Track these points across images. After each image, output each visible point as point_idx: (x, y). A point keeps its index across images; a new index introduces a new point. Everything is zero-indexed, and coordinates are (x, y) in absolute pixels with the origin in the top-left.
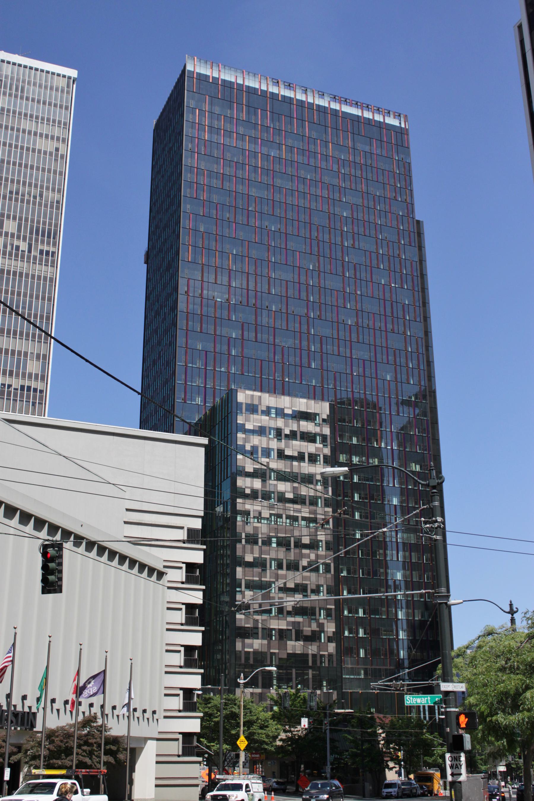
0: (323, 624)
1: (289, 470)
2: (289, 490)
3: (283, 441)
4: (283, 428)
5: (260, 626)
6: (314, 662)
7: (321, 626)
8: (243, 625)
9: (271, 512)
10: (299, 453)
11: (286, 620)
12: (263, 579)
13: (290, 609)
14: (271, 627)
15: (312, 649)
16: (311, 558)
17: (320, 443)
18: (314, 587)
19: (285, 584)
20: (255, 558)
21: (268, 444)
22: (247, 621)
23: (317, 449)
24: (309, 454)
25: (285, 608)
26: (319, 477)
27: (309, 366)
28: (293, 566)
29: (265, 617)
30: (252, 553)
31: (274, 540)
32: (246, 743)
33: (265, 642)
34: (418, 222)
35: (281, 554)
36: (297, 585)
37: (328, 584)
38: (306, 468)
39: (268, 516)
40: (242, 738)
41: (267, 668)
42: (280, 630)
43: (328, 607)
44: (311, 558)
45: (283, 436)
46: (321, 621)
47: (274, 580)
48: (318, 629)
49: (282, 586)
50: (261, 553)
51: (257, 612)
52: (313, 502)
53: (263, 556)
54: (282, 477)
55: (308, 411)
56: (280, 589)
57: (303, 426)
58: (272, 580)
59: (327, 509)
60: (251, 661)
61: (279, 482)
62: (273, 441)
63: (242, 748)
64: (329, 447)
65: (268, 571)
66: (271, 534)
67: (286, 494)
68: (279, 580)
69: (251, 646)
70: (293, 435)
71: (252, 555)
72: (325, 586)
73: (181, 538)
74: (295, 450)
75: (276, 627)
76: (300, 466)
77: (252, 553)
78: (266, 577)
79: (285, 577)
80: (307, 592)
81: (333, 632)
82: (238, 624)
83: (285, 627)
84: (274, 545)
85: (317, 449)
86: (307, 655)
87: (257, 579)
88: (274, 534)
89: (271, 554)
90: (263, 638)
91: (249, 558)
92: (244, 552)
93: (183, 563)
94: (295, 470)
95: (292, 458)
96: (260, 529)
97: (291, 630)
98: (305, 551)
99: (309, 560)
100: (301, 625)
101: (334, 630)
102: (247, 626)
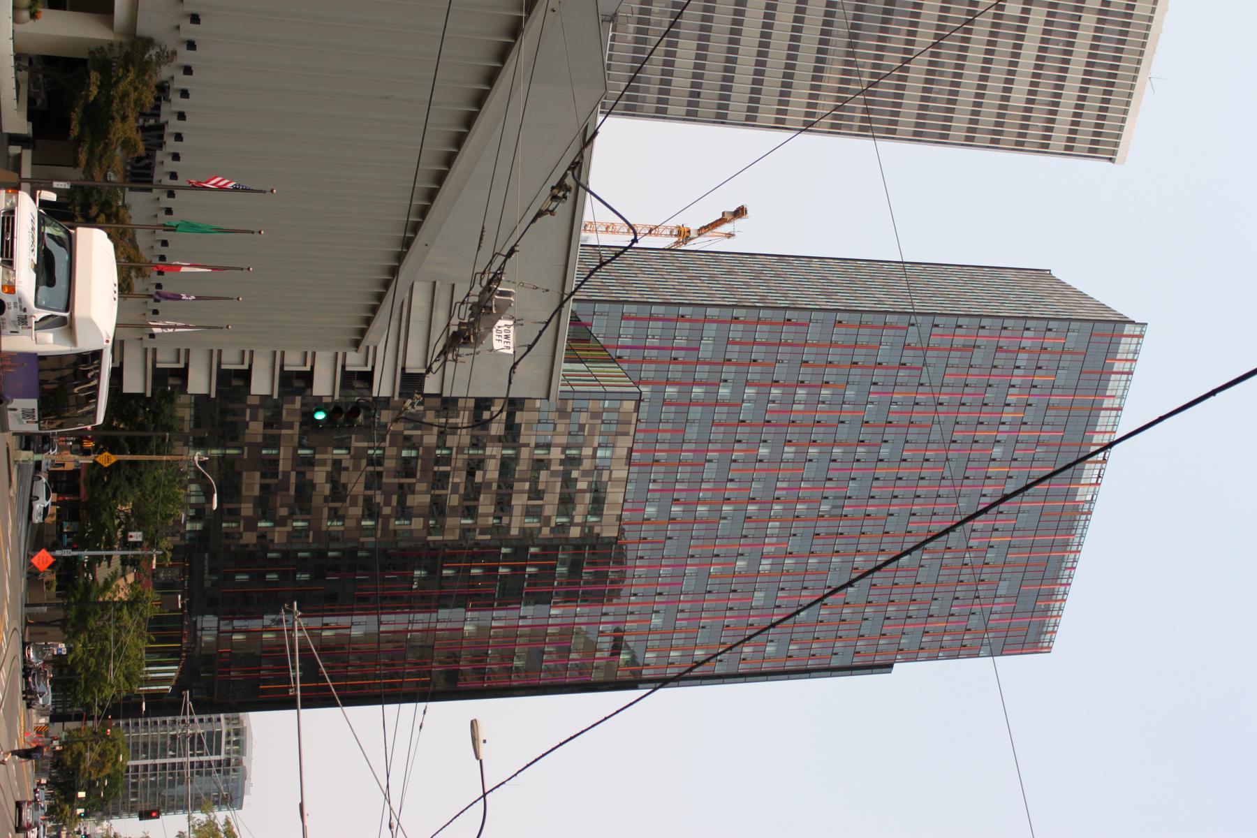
0: (285, 525)
1: (516, 477)
2: (487, 477)
3: (561, 468)
4: (581, 468)
5: (284, 432)
6: (230, 511)
7: (281, 522)
8: (286, 406)
9: (454, 449)
10: (543, 492)
11: (292, 470)
13: (308, 476)
14: (282, 449)
15: (247, 509)
17: (556, 523)
19: (347, 469)
21: (557, 445)
22: (290, 412)
23: (549, 518)
24: (541, 506)
25: (311, 468)
26: (505, 520)
27: (676, 501)
28: (374, 481)
29: (296, 439)
31: (414, 453)
32: (106, 465)
33: (259, 439)
34: (890, 666)
35: (390, 464)
36: (345, 486)
38: (519, 501)
39: (448, 444)
40: (114, 459)
41: (216, 495)
42: (277, 460)
45: (569, 468)
46: (289, 522)
47: (352, 453)
48: (277, 518)
49: (344, 464)
50: (395, 435)
52: (471, 512)
53: (388, 437)
54: (506, 466)
55: (606, 506)
57: (584, 498)
58: (352, 450)
59: (458, 531)
60: (230, 419)
61: (499, 462)
62: (562, 453)
63: (98, 460)
64: (552, 536)
66: (421, 449)
67: (482, 472)
68: (352, 461)
69: (254, 418)
70: (568, 482)
72: (342, 528)
73: (408, 364)
74: (547, 486)
75: (282, 456)
76: (522, 492)
80: (333, 501)
83: (281, 469)
84: (405, 453)
85: (549, 518)
86: (239, 502)
88: (421, 453)
89: (391, 448)
90: (265, 436)
93: (373, 367)
94: (517, 486)
95: (534, 481)
96: (429, 432)
97: (277, 477)
98: (395, 498)
99: (382, 504)
100: (283, 493)
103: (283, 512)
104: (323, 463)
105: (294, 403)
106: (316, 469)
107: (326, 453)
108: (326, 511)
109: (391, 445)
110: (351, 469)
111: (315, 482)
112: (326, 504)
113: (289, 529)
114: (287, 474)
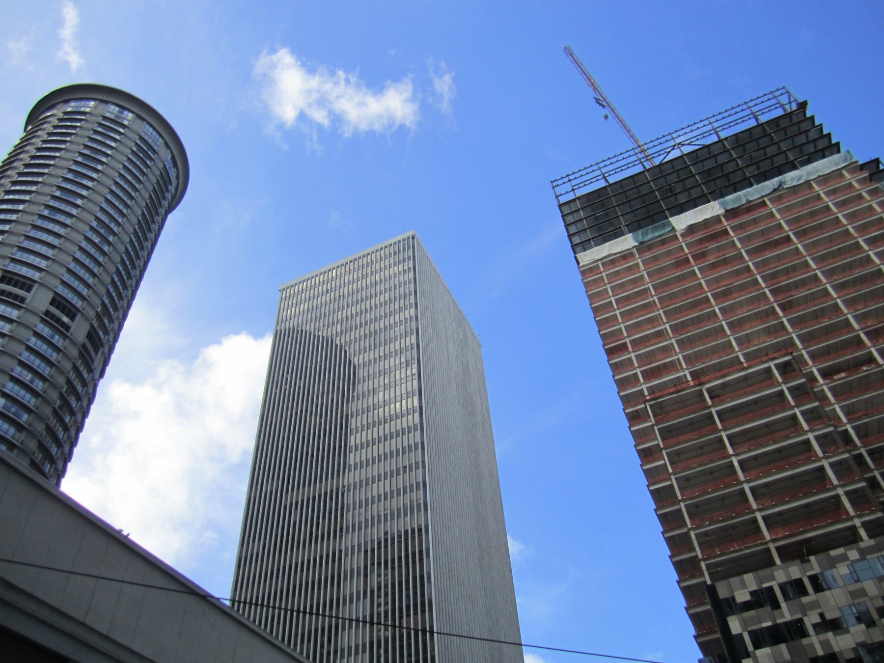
12: (779, 621)
16: (851, 558)
19: (822, 615)
20: (752, 593)
25: (839, 656)
30: (744, 586)
35: (795, 571)
44: (851, 558)
50: (760, 581)
53: (765, 585)
65: (783, 605)
68: (809, 613)
71: (746, 590)
77: (744, 586)
78: (783, 616)
79: (816, 605)
87: (769, 624)
89: (776, 577)
91: (742, 597)
92: (731, 590)
104: (825, 644)
107: (812, 645)
109: (774, 579)
110: (820, 611)
111: (854, 646)
112: (877, 623)
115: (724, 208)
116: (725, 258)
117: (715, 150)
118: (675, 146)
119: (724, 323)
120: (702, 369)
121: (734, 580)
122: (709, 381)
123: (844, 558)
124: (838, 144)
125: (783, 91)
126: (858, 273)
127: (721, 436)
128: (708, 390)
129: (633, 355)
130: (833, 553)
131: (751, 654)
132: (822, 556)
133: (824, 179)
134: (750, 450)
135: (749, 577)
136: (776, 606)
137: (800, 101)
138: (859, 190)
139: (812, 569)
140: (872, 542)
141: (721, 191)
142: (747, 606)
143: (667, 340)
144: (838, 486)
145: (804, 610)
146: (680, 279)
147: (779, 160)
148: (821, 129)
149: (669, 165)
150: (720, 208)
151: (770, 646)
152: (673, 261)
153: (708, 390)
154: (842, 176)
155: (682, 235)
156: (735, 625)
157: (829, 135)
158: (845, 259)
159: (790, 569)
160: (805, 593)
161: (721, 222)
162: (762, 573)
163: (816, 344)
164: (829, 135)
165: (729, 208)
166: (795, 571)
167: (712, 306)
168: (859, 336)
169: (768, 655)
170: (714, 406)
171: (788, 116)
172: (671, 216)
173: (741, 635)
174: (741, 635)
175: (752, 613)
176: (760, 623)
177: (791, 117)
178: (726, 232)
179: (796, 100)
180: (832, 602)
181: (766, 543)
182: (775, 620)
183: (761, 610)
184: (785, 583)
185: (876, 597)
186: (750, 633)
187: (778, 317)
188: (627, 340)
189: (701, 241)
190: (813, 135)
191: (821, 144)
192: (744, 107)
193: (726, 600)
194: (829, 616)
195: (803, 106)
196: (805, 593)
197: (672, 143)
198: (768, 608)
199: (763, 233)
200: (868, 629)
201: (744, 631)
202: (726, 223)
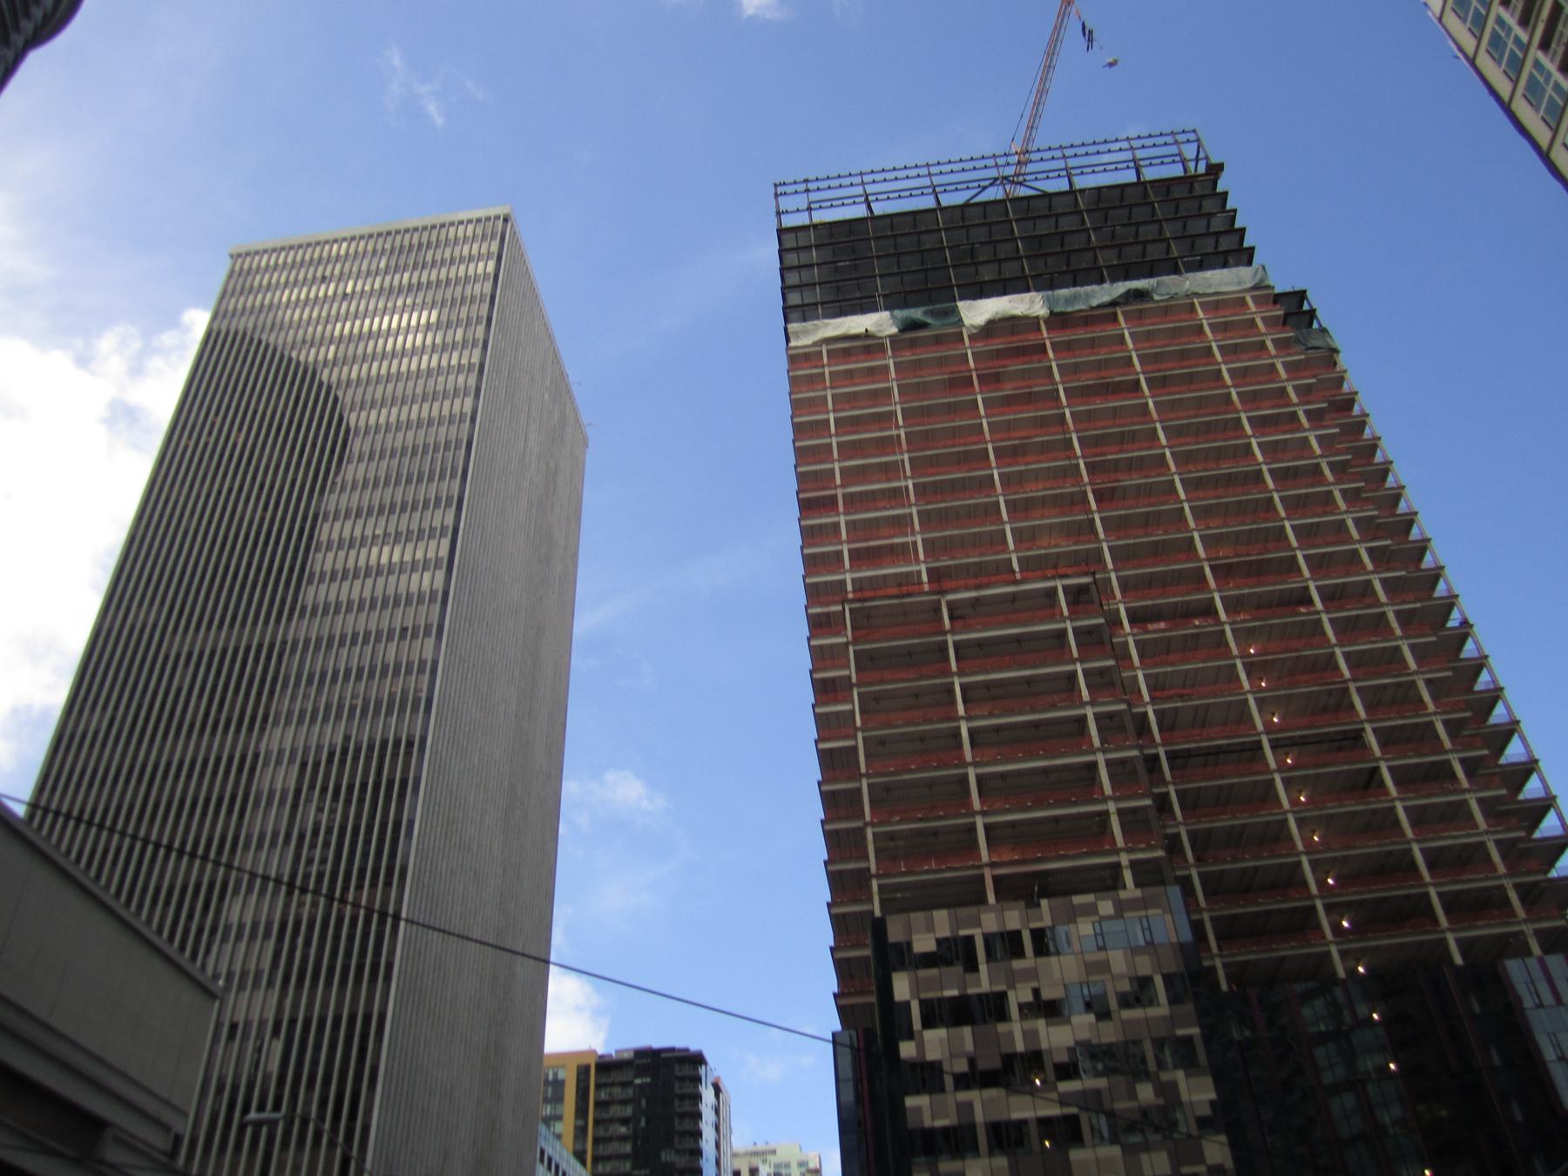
5: (979, 1117)
7: (1168, 1092)
8: (928, 1122)
11: (1056, 1089)
12: (971, 991)
13: (1063, 1058)
18: (1125, 986)
19: (1036, 992)
20: (939, 942)
25: (1046, 1058)
29: (992, 1093)
30: (930, 927)
35: (1013, 919)
37: (1165, 971)
43: (1180, 1032)
48: (1161, 1101)
49: (1028, 997)
50: (956, 924)
51: (963, 1082)
53: (963, 933)
56: (1027, 1010)
65: (983, 967)
68: (1018, 985)
72: (1159, 981)
77: (930, 927)
78: (978, 984)
79: (1033, 974)
81: (1212, 1103)
82: (911, 1122)
83: (1055, 1111)
87: (954, 992)
90: (991, 1154)
91: (924, 944)
101: (1213, 1096)
102: (939, 1123)
103: (1146, 1092)
104: (1031, 1036)
105: (918, 1110)
106: (1044, 1045)
108: (1128, 1014)
109: (980, 925)
110: (1035, 984)
111: (1071, 1043)
112: (1114, 1015)
113: (1180, 1075)
114: (1064, 1100)
115: (1050, 308)
116: (1030, 393)
117: (1060, 206)
118: (996, 179)
119: (1001, 499)
120: (949, 567)
121: (917, 917)
122: (955, 590)
123: (1091, 910)
124: (1251, 250)
125: (1192, 137)
126: (1227, 468)
127: (953, 683)
128: (949, 604)
129: (842, 519)
130: (1078, 900)
131: (916, 1036)
132: (1058, 901)
133: (1217, 304)
134: (991, 715)
135: (941, 916)
136: (972, 966)
137: (1214, 160)
138: (1262, 335)
139: (1041, 919)
140: (1138, 893)
141: (1052, 279)
142: (928, 960)
143: (903, 506)
144: (1110, 798)
145: (1012, 979)
146: (951, 409)
147: (1155, 252)
148: (1233, 219)
149: (910, 218)
150: (1042, 307)
151: (947, 1026)
152: (946, 377)
153: (949, 604)
154: (1114, 319)
155: (972, 337)
156: (902, 987)
157: (1243, 231)
158: (1215, 440)
159: (1007, 914)
160: (1019, 953)
161: (1039, 330)
162: (964, 912)
163: (1135, 568)
164: (1243, 231)
165: (1057, 310)
166: (1013, 919)
167: (989, 467)
168: (1202, 568)
169: (941, 1040)
170: (953, 631)
171: (1188, 180)
172: (961, 299)
173: (906, 1005)
174: (907, 1004)
175: (933, 972)
176: (942, 989)
177: (1192, 184)
178: (1042, 349)
179: (1207, 158)
180: (1057, 975)
181: (980, 867)
182: (965, 986)
183: (946, 970)
184: (994, 935)
185: (1121, 977)
186: (922, 1003)
187: (1088, 511)
188: (840, 492)
189: (999, 354)
190: (1217, 224)
191: (1226, 243)
192: (1058, 154)
193: (896, 945)
194: (1046, 995)
195: (1215, 170)
196: (1019, 953)
197: (993, 173)
198: (959, 969)
199: (1100, 365)
200: (1100, 1024)
201: (913, 997)
202: (1045, 335)
